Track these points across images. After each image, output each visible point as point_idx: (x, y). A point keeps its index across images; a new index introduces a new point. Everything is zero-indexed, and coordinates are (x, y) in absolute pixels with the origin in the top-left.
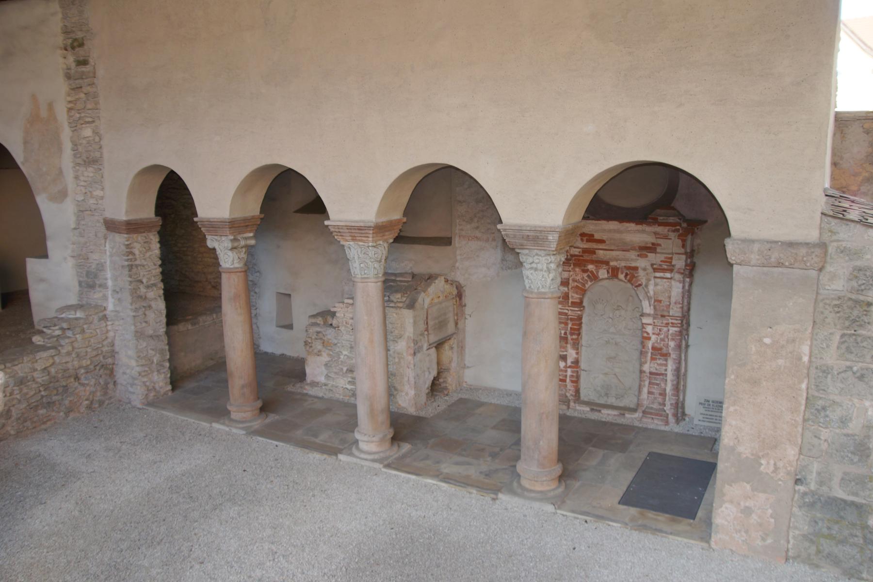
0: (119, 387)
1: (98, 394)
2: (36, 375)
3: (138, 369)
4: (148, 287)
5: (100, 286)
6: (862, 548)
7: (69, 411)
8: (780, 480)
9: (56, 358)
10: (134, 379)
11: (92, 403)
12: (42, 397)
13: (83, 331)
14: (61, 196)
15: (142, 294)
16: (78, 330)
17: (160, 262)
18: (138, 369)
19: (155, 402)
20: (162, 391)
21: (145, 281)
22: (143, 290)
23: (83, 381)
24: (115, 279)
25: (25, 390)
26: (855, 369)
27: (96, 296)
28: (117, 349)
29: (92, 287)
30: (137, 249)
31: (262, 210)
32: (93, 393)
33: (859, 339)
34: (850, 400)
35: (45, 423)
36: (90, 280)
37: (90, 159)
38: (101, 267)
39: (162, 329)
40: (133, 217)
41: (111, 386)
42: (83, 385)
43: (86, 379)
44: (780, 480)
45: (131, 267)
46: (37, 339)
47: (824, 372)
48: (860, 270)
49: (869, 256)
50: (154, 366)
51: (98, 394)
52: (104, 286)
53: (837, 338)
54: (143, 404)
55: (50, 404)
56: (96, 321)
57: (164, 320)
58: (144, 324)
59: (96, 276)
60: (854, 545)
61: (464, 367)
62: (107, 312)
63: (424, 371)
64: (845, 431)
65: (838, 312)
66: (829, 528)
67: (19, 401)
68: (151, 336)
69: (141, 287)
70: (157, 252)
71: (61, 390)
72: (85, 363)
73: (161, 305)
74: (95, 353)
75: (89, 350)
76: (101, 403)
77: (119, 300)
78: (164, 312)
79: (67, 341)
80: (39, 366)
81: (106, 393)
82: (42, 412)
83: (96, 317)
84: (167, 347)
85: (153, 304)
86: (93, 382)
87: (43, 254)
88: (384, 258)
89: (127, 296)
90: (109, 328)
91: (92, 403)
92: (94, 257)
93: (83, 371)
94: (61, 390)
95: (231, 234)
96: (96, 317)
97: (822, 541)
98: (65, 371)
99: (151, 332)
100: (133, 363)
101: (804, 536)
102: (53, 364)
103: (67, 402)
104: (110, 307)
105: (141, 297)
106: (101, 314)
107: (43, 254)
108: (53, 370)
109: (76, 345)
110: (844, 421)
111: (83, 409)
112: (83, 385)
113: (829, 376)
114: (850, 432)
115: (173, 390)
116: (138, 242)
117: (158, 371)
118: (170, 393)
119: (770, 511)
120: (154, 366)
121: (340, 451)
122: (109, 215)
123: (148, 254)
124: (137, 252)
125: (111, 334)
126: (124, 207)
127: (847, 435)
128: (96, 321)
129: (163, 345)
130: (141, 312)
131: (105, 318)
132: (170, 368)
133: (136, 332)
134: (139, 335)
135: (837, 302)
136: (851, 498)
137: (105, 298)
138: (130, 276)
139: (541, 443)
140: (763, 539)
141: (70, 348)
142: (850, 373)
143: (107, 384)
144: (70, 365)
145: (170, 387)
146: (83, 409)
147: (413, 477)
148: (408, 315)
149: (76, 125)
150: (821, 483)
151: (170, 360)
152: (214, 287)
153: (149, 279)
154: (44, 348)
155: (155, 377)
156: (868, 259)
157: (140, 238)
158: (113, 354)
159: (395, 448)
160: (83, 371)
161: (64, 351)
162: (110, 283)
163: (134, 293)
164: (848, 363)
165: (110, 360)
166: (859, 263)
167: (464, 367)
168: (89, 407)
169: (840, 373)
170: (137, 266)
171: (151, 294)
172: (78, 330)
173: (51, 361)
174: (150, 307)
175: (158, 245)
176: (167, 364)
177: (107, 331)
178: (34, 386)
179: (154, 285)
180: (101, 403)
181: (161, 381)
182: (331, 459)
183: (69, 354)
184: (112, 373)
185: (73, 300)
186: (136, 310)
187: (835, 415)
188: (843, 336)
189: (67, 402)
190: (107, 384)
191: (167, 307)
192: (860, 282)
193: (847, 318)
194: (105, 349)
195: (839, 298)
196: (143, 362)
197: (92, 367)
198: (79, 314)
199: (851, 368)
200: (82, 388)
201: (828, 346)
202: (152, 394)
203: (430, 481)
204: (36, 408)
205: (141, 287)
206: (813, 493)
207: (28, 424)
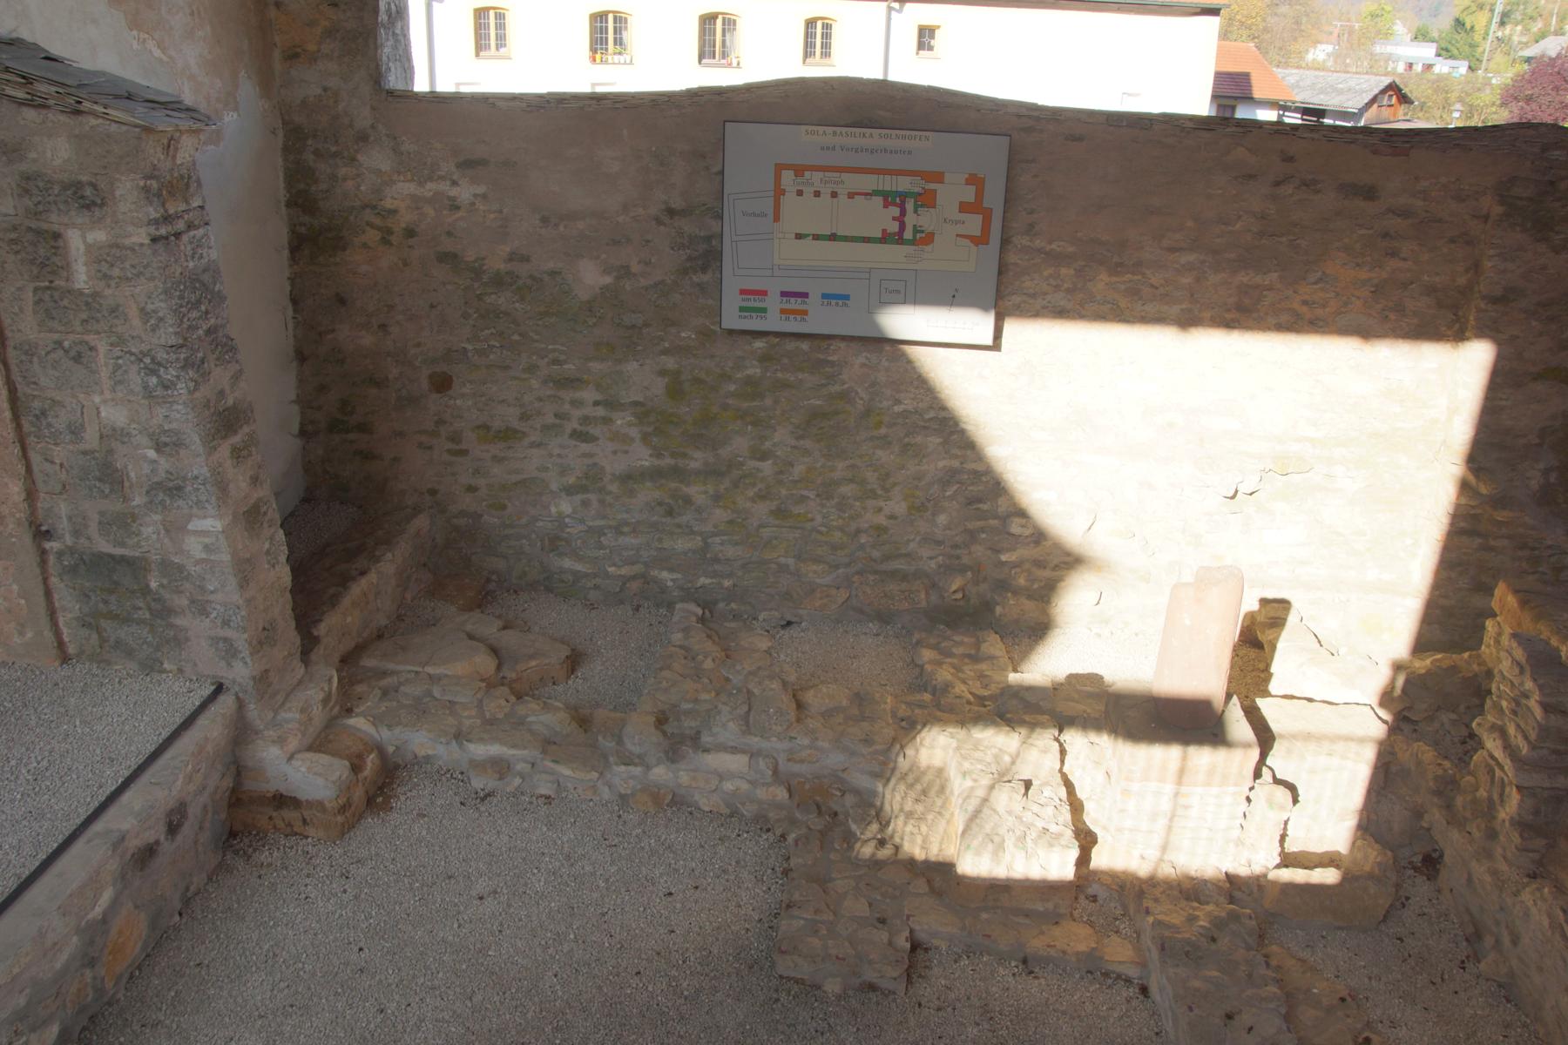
6: (152, 626)
8: (11, 535)
26: (66, 344)
33: (56, 295)
34: (74, 396)
44: (11, 535)
47: (26, 353)
48: (28, 178)
49: (33, 155)
53: (29, 296)
60: (140, 622)
64: (82, 447)
65: (17, 252)
66: (106, 602)
97: (104, 623)
101: (77, 619)
110: (76, 431)
113: (35, 359)
114: (87, 447)
119: (15, 587)
127: (85, 453)
135: (13, 236)
136: (118, 551)
140: (22, 634)
142: (60, 352)
150: (76, 533)
156: (35, 161)
164: (56, 336)
166: (23, 167)
169: (48, 353)
187: (60, 421)
188: (36, 290)
192: (35, 199)
193: (32, 262)
195: (15, 228)
199: (59, 343)
201: (21, 310)
206: (72, 551)
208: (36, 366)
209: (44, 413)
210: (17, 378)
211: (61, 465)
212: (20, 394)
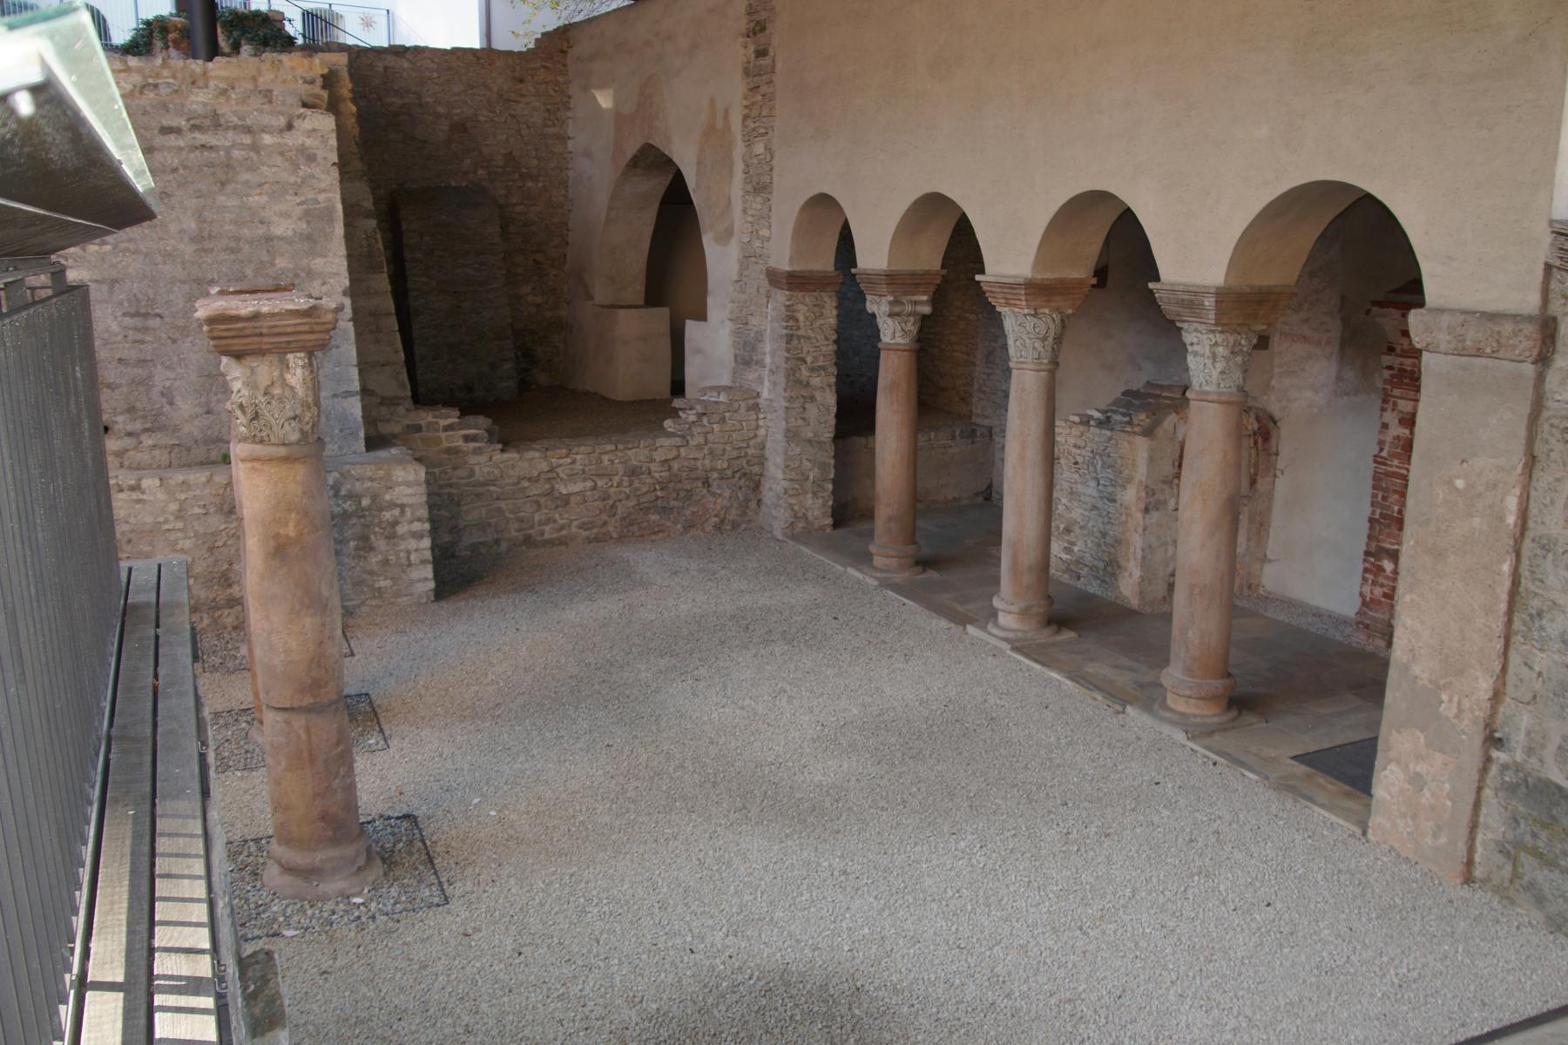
0: (763, 508)
1: (734, 512)
2: (653, 467)
3: (785, 484)
4: (812, 370)
5: (757, 362)
7: (689, 526)
9: (682, 450)
10: (779, 498)
11: (722, 521)
12: (657, 498)
13: (723, 420)
14: (725, 236)
15: (804, 378)
16: (716, 418)
17: (835, 337)
18: (785, 484)
19: (801, 532)
20: (817, 524)
21: (809, 360)
22: (805, 373)
23: (714, 488)
24: (773, 355)
25: (636, 484)
27: (751, 376)
28: (767, 453)
29: (747, 363)
30: (802, 313)
31: (943, 267)
32: (727, 509)
35: (656, 533)
36: (746, 357)
37: (760, 188)
38: (759, 337)
39: (828, 434)
40: (797, 268)
41: (753, 505)
42: (714, 494)
43: (719, 487)
45: (789, 338)
46: (668, 423)
50: (809, 484)
51: (734, 512)
52: (760, 363)
54: (785, 535)
55: (665, 511)
56: (743, 410)
57: (833, 422)
58: (800, 422)
59: (754, 349)
61: (1265, 560)
62: (761, 401)
63: (1165, 544)
67: (628, 497)
68: (810, 441)
69: (803, 368)
70: (833, 321)
71: (682, 494)
72: (721, 464)
73: (830, 399)
74: (735, 454)
75: (728, 448)
76: (735, 526)
77: (775, 384)
78: (834, 409)
79: (699, 430)
80: (659, 456)
81: (744, 513)
82: (654, 517)
83: (743, 404)
84: (832, 462)
85: (818, 395)
86: (727, 493)
87: (702, 316)
88: (1052, 334)
89: (781, 378)
90: (761, 423)
91: (722, 521)
92: (754, 321)
93: (716, 475)
94: (682, 494)
95: (892, 293)
96: (743, 404)
98: (691, 470)
99: (810, 435)
100: (780, 476)
102: (677, 457)
103: (688, 513)
104: (765, 394)
105: (799, 382)
106: (751, 402)
107: (702, 316)
108: (675, 466)
109: (711, 437)
111: (708, 528)
112: (714, 494)
115: (836, 525)
116: (804, 305)
117: (814, 493)
118: (828, 530)
120: (809, 484)
121: (972, 621)
122: (773, 263)
123: (818, 323)
124: (801, 318)
125: (762, 432)
126: (787, 253)
128: (743, 410)
129: (827, 455)
130: (797, 404)
131: (756, 408)
132: (833, 492)
133: (788, 430)
134: (792, 435)
137: (760, 380)
138: (788, 350)
139: (1190, 634)
141: (702, 440)
143: (747, 501)
144: (699, 464)
145: (829, 521)
146: (708, 528)
147: (1038, 667)
148: (1142, 445)
149: (749, 144)
151: (834, 481)
152: (963, 399)
153: (815, 359)
154: (673, 435)
155: (809, 501)
157: (808, 298)
158: (761, 460)
159: (1047, 631)
160: (716, 475)
161: (692, 443)
162: (768, 360)
163: (791, 374)
165: (756, 469)
167: (1265, 560)
168: (718, 527)
170: (799, 338)
171: (816, 381)
172: (716, 418)
173: (674, 453)
174: (812, 398)
175: (835, 312)
176: (830, 487)
177: (758, 427)
178: (649, 481)
179: (823, 368)
180: (735, 526)
181: (818, 508)
182: (956, 629)
183: (699, 447)
184: (757, 487)
185: (725, 380)
186: (790, 399)
189: (688, 513)
190: (747, 501)
191: (839, 404)
194: (750, 451)
196: (793, 475)
197: (729, 472)
198: (723, 398)
200: (712, 499)
202: (800, 525)
203: (1054, 675)
204: (647, 510)
205: (803, 368)
207: (635, 528)
208: (1548, 564)
209: (1540, 614)
210: (1524, 571)
211: (1540, 674)
212: (1521, 589)
